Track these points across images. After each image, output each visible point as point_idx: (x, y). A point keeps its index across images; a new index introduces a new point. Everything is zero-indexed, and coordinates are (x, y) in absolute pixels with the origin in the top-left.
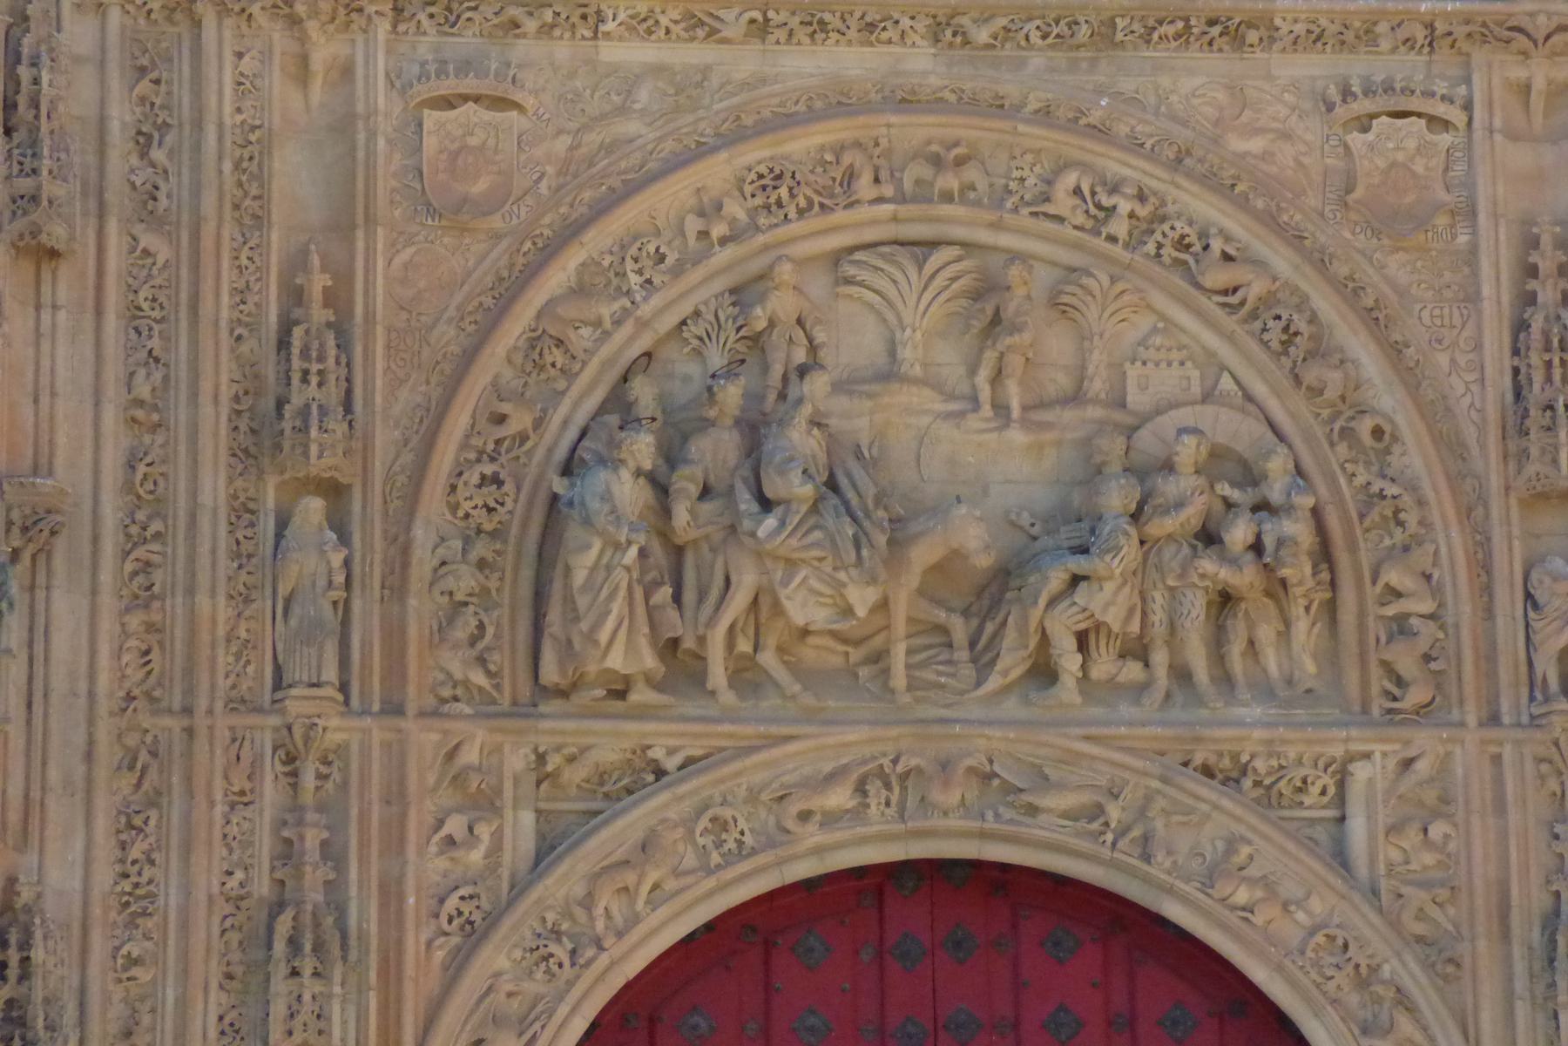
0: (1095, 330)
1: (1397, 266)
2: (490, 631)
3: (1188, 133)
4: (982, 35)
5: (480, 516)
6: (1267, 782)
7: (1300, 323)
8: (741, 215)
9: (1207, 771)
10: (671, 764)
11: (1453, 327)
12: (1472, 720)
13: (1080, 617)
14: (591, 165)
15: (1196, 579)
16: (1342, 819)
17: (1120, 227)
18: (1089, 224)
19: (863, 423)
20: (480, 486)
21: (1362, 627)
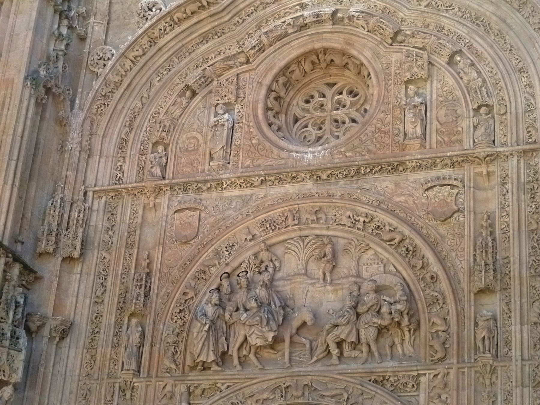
0: (354, 255)
1: (442, 229)
2: (179, 353)
3: (383, 197)
4: (324, 176)
5: (179, 321)
6: (395, 385)
7: (411, 248)
8: (258, 233)
9: (376, 382)
10: (223, 388)
11: (457, 245)
12: (455, 361)
13: (335, 337)
14: (218, 223)
15: (372, 324)
16: (418, 395)
17: (360, 225)
18: (352, 225)
19: (288, 288)
20: (179, 313)
21: (426, 336)
